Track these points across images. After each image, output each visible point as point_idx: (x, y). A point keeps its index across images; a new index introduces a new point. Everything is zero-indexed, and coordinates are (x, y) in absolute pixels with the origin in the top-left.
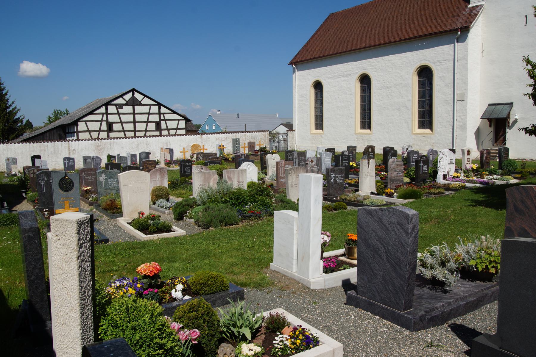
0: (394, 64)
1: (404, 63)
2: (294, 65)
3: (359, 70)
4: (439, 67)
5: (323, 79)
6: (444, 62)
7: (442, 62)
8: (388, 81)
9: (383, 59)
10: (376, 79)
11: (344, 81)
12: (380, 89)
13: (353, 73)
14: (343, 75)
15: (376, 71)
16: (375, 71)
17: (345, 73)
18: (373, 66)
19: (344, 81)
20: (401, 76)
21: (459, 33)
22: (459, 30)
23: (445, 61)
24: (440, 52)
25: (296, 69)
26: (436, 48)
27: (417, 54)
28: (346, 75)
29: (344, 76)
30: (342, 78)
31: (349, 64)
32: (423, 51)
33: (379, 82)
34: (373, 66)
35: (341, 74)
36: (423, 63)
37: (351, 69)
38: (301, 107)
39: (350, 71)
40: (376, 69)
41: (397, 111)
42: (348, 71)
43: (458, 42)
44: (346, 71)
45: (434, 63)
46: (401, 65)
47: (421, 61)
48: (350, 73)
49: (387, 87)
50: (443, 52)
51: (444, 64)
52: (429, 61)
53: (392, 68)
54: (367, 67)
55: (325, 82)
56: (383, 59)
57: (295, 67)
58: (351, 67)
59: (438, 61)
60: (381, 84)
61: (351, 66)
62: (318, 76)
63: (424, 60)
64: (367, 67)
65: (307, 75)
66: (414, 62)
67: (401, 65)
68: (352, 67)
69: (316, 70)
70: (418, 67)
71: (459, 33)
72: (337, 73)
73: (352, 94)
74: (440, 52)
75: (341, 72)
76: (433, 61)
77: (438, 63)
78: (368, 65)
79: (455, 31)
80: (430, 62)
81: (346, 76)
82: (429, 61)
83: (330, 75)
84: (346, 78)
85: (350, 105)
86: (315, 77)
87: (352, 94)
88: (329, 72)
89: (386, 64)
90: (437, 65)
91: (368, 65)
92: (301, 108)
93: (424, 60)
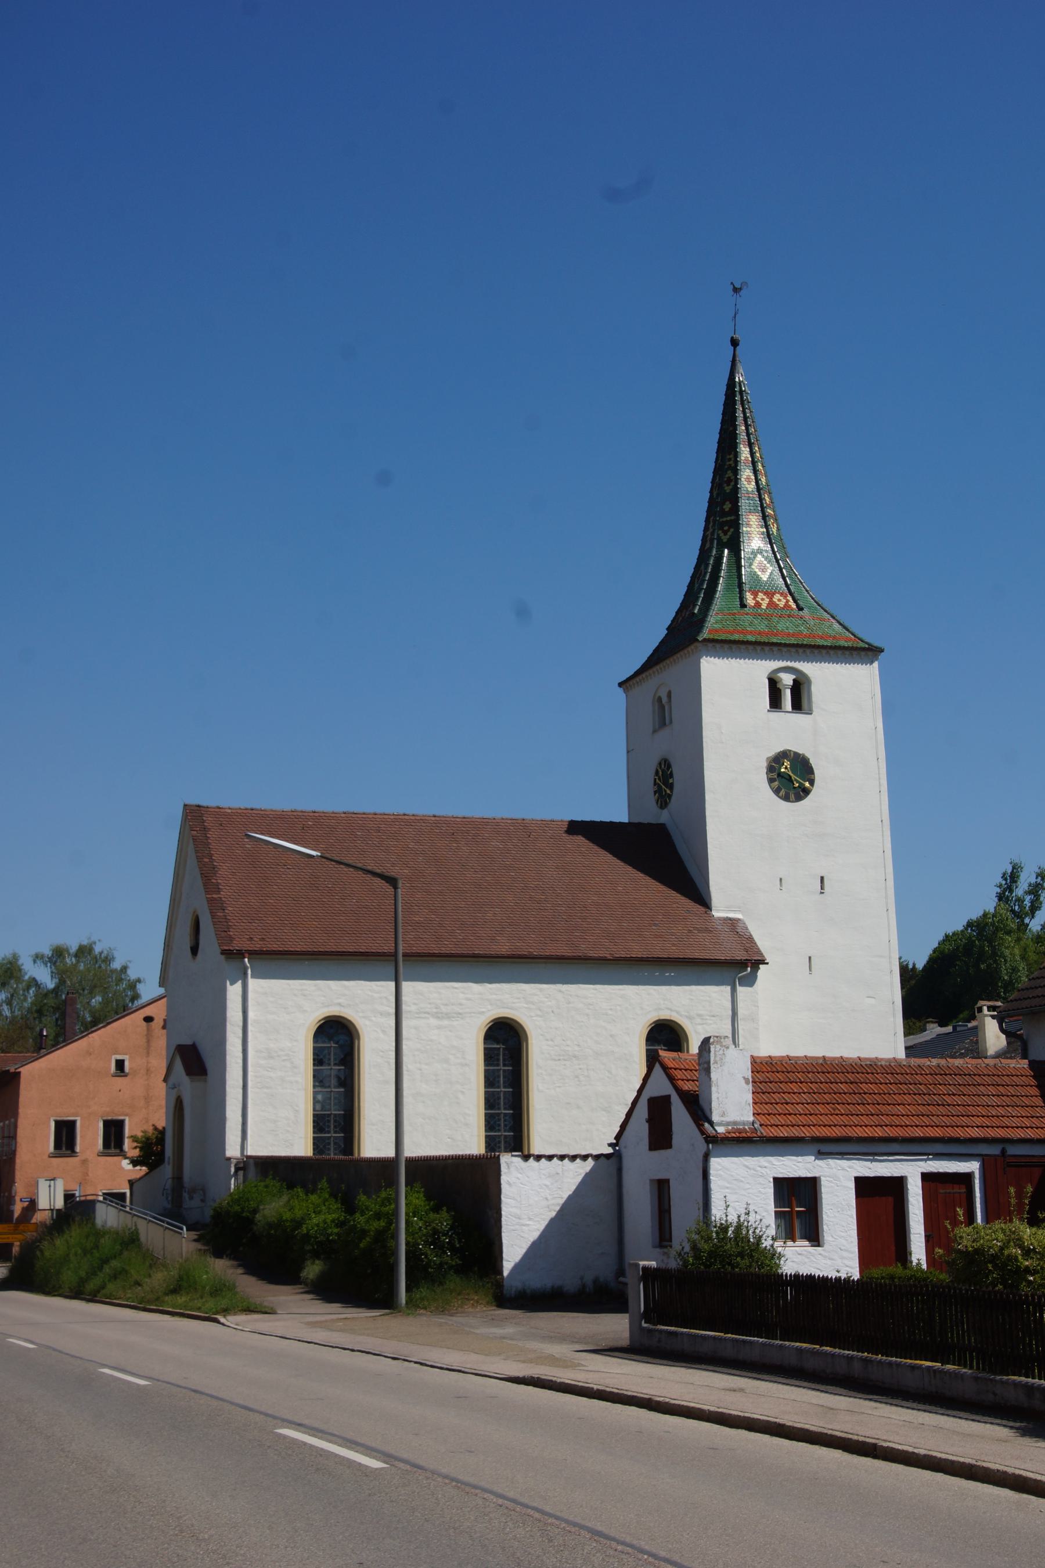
0: (591, 1007)
1: (618, 1007)
2: (246, 960)
3: (489, 1007)
4: (699, 1027)
5: (361, 1014)
6: (710, 1020)
7: (706, 1019)
8: (576, 1043)
9: (560, 991)
10: (542, 1035)
11: (439, 1028)
12: (555, 1060)
13: (467, 1010)
14: (437, 1013)
15: (541, 1016)
16: (537, 1016)
17: (444, 1009)
18: (533, 1003)
19: (439, 1028)
20: (611, 1036)
21: (749, 969)
22: (750, 964)
23: (713, 1018)
24: (702, 998)
25: (249, 972)
26: (694, 987)
27: (649, 994)
28: (446, 1014)
29: (440, 1015)
30: (433, 1021)
31: (456, 988)
32: (664, 989)
33: (550, 1043)
34: (533, 1003)
35: (427, 1010)
36: (665, 1015)
37: (464, 1002)
38: (267, 1088)
39: (461, 1004)
40: (540, 1010)
41: (603, 1112)
42: (452, 1005)
43: (740, 985)
44: (446, 1005)
45: (690, 1018)
46: (610, 1012)
47: (660, 1009)
48: (460, 1011)
49: (575, 1056)
50: (708, 999)
51: (711, 1024)
52: (678, 1012)
53: (588, 1015)
54: (514, 1003)
55: (367, 1023)
56: (560, 991)
57: (248, 965)
58: (461, 996)
59: (699, 1015)
60: (556, 1048)
61: (463, 993)
62: (340, 1004)
63: (668, 1009)
64: (514, 1003)
65: (295, 995)
66: (642, 1009)
67: (610, 1012)
68: (469, 996)
69: (334, 985)
70: (652, 1022)
71: (749, 969)
72: (415, 1004)
73: (466, 1065)
74: (702, 998)
75: (430, 1004)
76: (686, 1014)
77: (698, 1020)
78: (519, 998)
79: (742, 964)
80: (681, 1016)
81: (448, 1016)
82: (678, 1012)
83: (388, 1008)
84: (446, 1022)
85: (463, 1092)
86: (328, 1006)
87: (466, 1065)
88: (386, 998)
89: (569, 1003)
90: (696, 1024)
91: (519, 998)
92: (265, 1090)
93: (668, 1009)
